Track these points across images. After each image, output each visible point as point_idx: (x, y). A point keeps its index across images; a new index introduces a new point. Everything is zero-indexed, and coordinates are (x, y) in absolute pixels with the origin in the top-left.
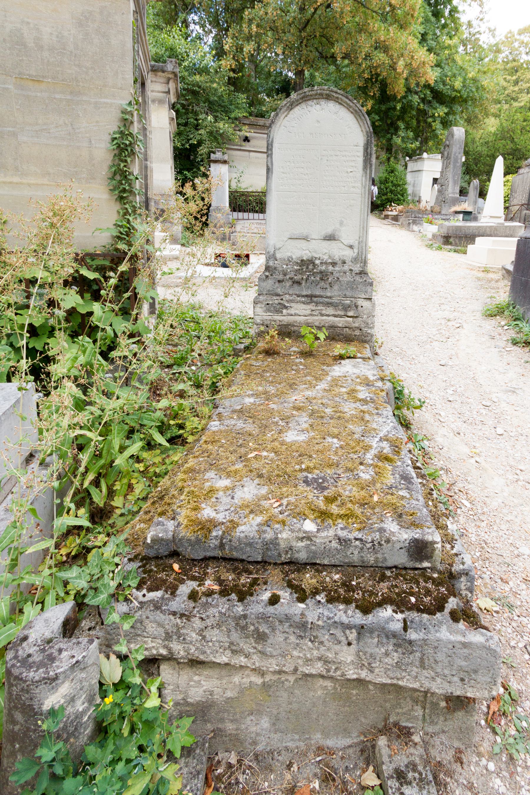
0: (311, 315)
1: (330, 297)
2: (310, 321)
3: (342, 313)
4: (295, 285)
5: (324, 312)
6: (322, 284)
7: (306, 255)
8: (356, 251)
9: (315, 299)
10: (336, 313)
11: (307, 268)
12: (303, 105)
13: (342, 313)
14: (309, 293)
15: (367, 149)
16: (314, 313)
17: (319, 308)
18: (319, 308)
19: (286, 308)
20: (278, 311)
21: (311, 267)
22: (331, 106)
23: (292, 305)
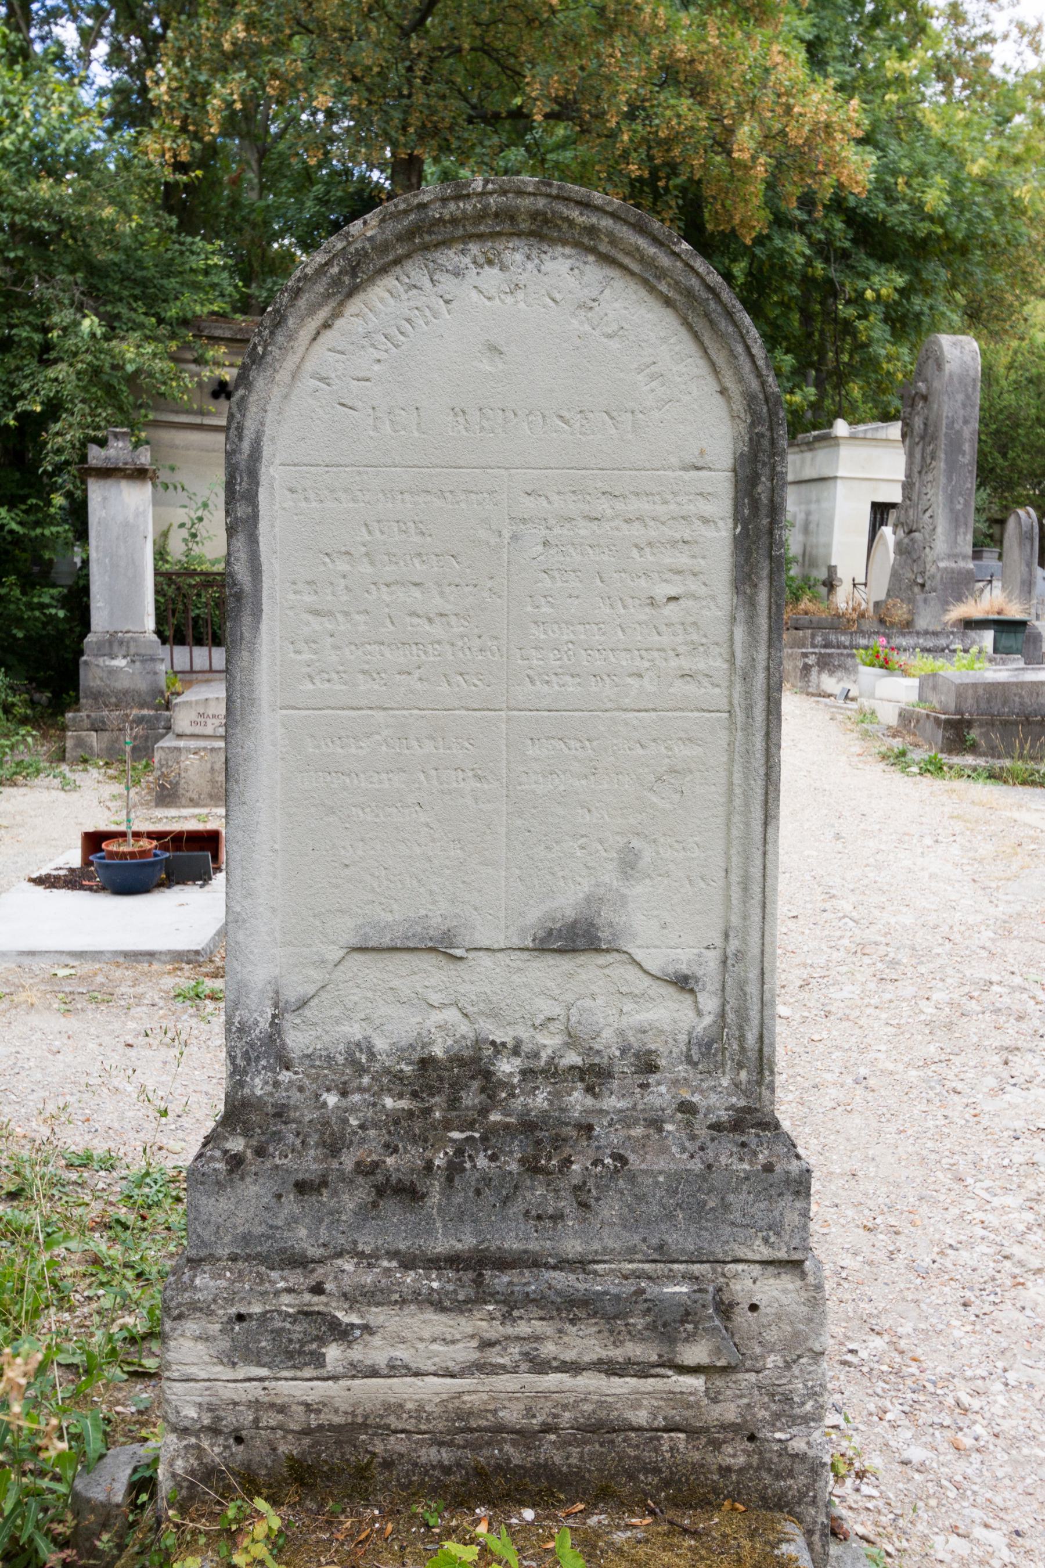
1: (581, 1264)
3: (645, 1352)
4: (390, 1206)
5: (548, 1349)
6: (537, 1193)
7: (444, 1031)
8: (709, 1003)
9: (500, 1281)
10: (617, 1354)
11: (453, 1102)
12: (415, 271)
13: (645, 1352)
14: (466, 1242)
15: (753, 480)
17: (523, 1328)
18: (523, 1328)
20: (302, 1356)
21: (471, 1098)
22: (561, 271)
23: (377, 1316)
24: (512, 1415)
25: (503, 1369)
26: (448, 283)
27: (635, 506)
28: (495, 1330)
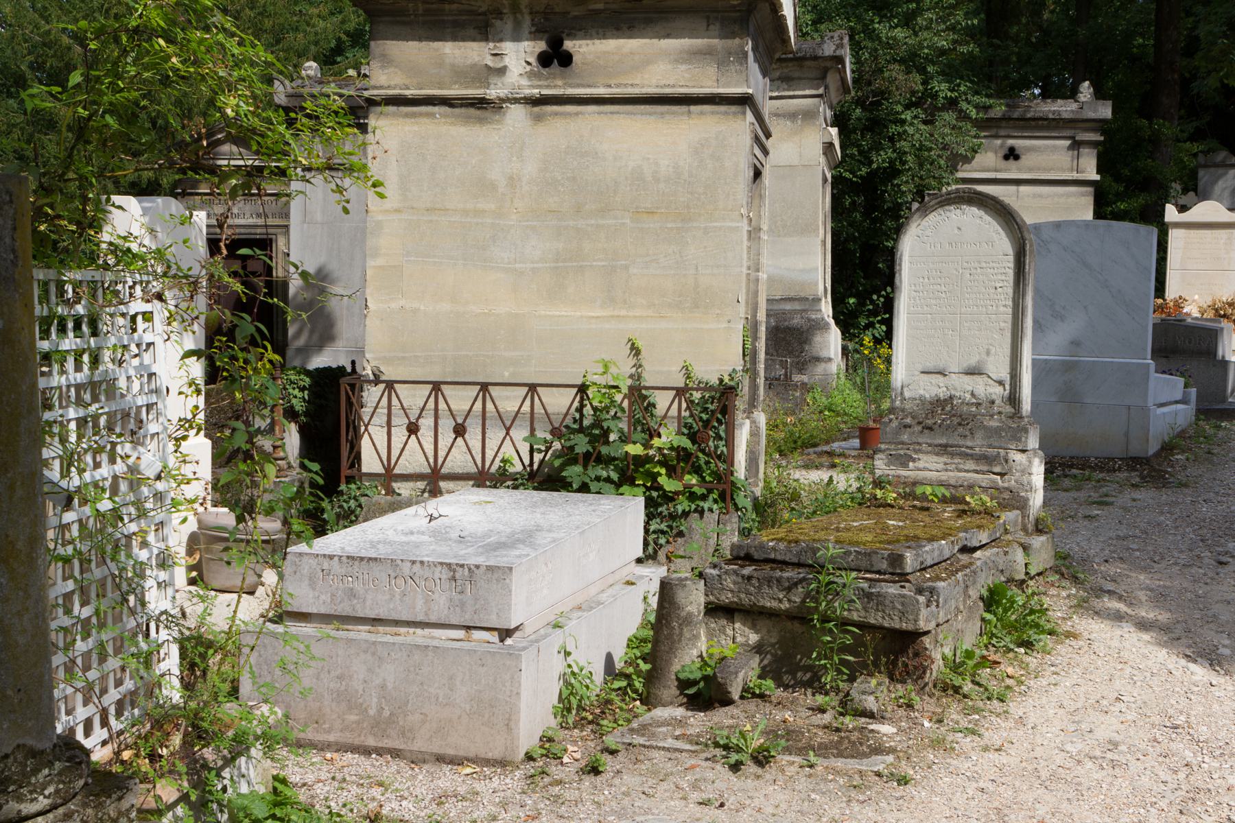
0: (946, 470)
1: (971, 448)
3: (985, 468)
6: (961, 429)
7: (942, 393)
8: (1008, 387)
12: (940, 211)
13: (985, 468)
16: (948, 467)
19: (914, 460)
21: (948, 408)
22: (974, 210)
23: (921, 456)
24: (952, 482)
28: (949, 461)
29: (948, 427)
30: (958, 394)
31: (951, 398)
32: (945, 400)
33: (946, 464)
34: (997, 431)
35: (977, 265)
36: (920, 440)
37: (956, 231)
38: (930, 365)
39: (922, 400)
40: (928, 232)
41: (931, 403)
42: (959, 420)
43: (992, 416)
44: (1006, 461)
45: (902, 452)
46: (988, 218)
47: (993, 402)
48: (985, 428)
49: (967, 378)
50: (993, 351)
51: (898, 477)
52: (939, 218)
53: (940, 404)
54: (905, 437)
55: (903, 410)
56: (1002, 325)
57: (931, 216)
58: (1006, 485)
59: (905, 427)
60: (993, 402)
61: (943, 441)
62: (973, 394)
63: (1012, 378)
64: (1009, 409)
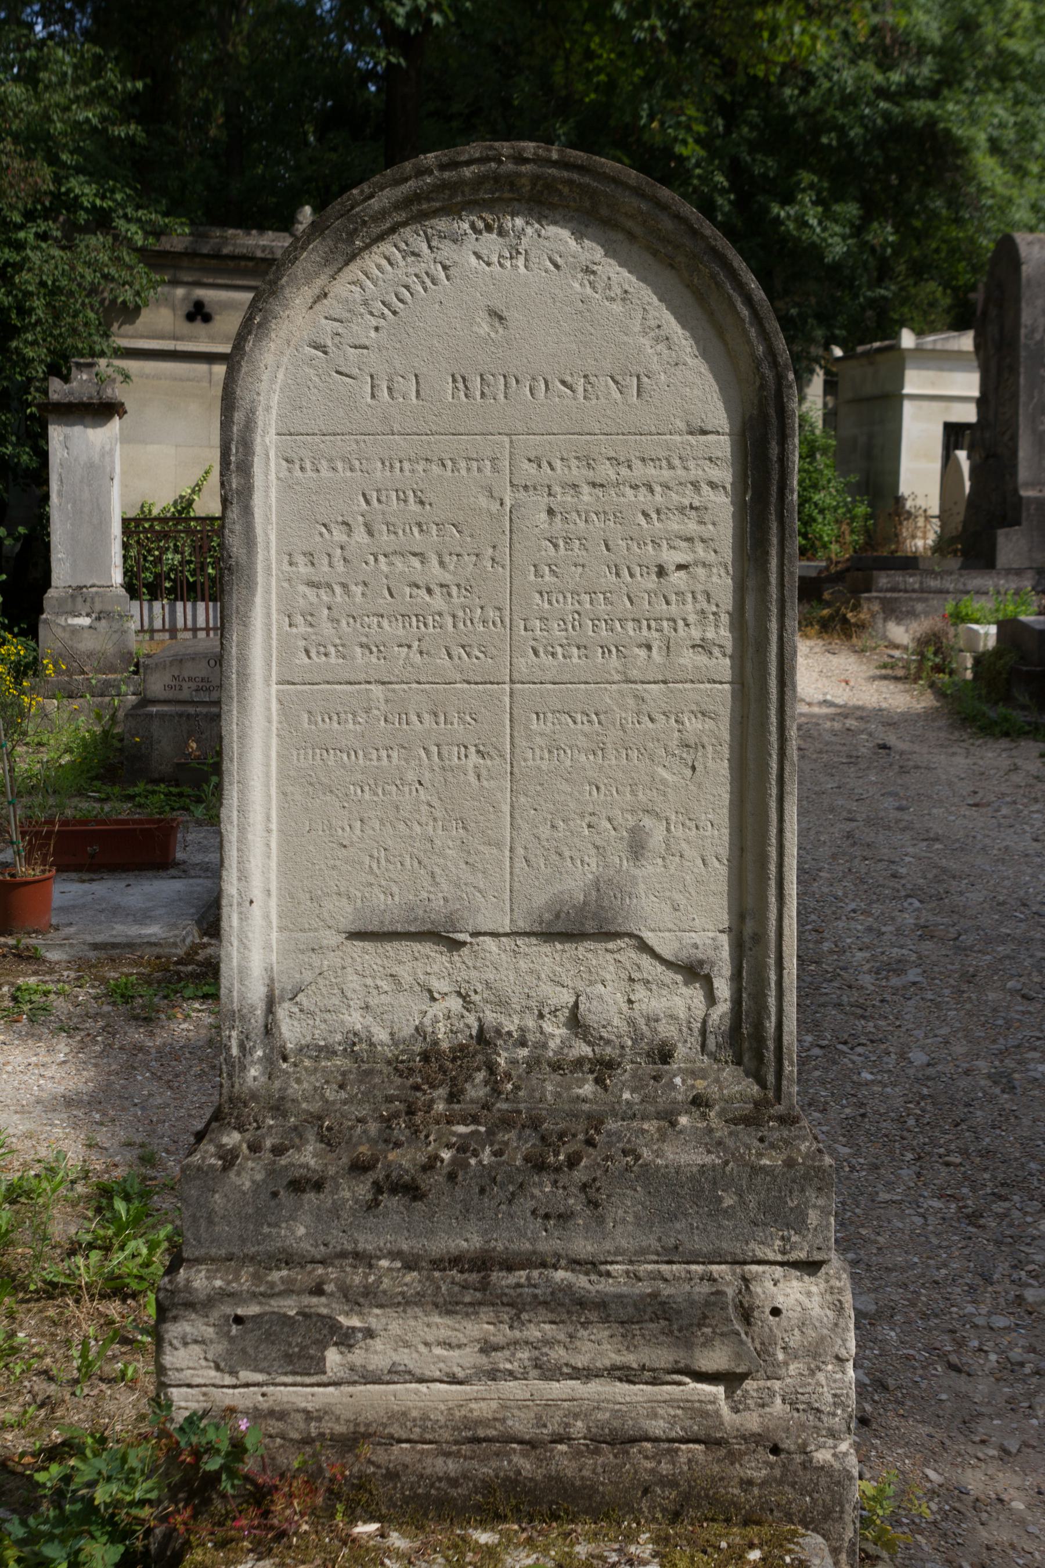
0: (493, 1374)
1: (591, 1266)
2: (483, 1409)
3: (662, 1357)
4: (391, 1202)
5: (558, 1354)
6: (543, 1188)
7: (445, 1020)
8: (723, 988)
10: (631, 1359)
11: (453, 1097)
17: (533, 1333)
18: (533, 1333)
21: (476, 1090)
22: (560, 237)
23: (376, 1318)
24: (521, 1424)
25: (511, 1375)
26: (447, 250)
27: (641, 472)
28: (503, 1333)
29: (489, 1179)
30: (510, 1025)
31: (484, 1038)
32: (460, 1052)
33: (488, 1348)
34: (700, 1190)
35: (577, 473)
36: (366, 1243)
37: (484, 327)
38: (387, 904)
39: (355, 1046)
40: (363, 329)
41: (400, 1068)
42: (530, 1143)
43: (669, 1117)
44: (747, 1315)
45: (290, 1307)
46: (617, 274)
47: (664, 1054)
48: (648, 1175)
49: (548, 958)
50: (657, 835)
51: (281, 1415)
52: (405, 269)
53: (442, 1070)
54: (298, 1233)
55: (279, 1107)
56: (693, 725)
57: (373, 260)
58: (752, 1422)
59: (297, 1186)
60: (664, 1054)
61: (469, 1241)
62: (575, 1022)
63: (739, 948)
64: (734, 1085)
